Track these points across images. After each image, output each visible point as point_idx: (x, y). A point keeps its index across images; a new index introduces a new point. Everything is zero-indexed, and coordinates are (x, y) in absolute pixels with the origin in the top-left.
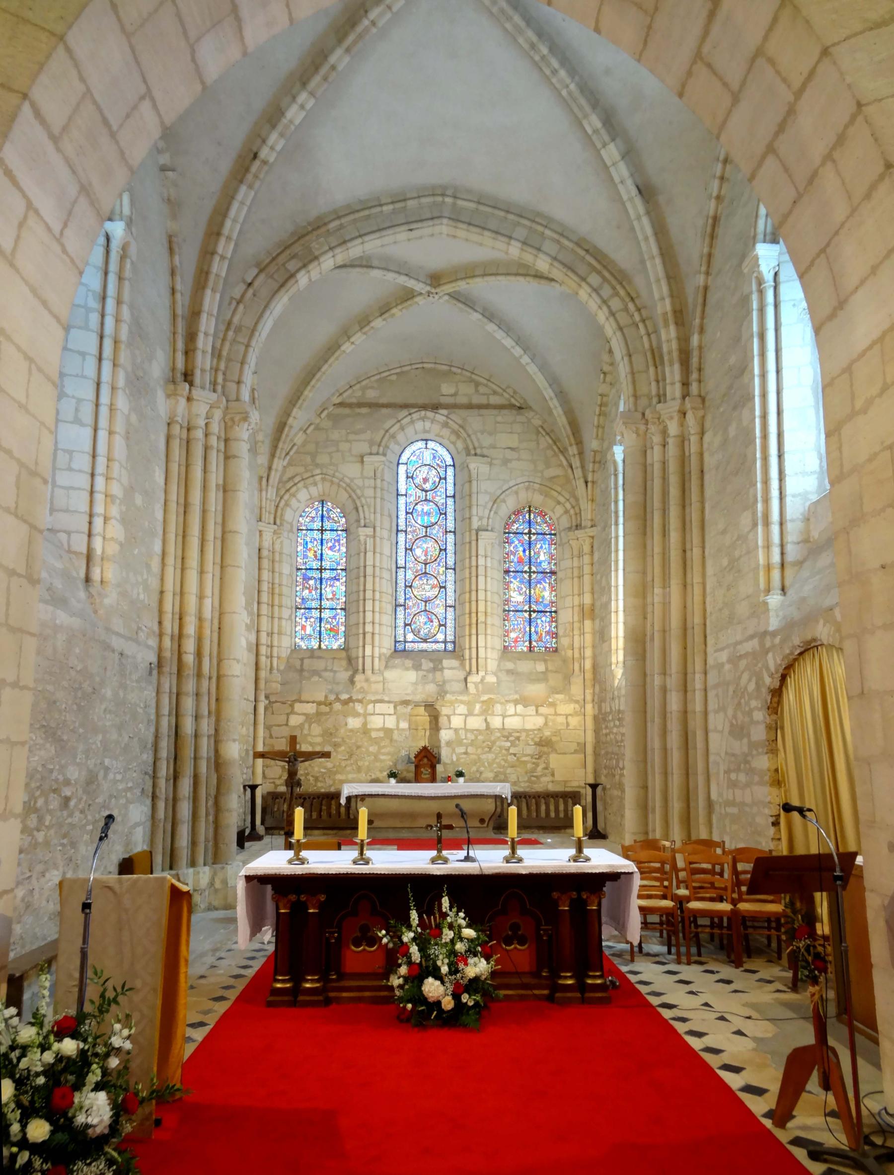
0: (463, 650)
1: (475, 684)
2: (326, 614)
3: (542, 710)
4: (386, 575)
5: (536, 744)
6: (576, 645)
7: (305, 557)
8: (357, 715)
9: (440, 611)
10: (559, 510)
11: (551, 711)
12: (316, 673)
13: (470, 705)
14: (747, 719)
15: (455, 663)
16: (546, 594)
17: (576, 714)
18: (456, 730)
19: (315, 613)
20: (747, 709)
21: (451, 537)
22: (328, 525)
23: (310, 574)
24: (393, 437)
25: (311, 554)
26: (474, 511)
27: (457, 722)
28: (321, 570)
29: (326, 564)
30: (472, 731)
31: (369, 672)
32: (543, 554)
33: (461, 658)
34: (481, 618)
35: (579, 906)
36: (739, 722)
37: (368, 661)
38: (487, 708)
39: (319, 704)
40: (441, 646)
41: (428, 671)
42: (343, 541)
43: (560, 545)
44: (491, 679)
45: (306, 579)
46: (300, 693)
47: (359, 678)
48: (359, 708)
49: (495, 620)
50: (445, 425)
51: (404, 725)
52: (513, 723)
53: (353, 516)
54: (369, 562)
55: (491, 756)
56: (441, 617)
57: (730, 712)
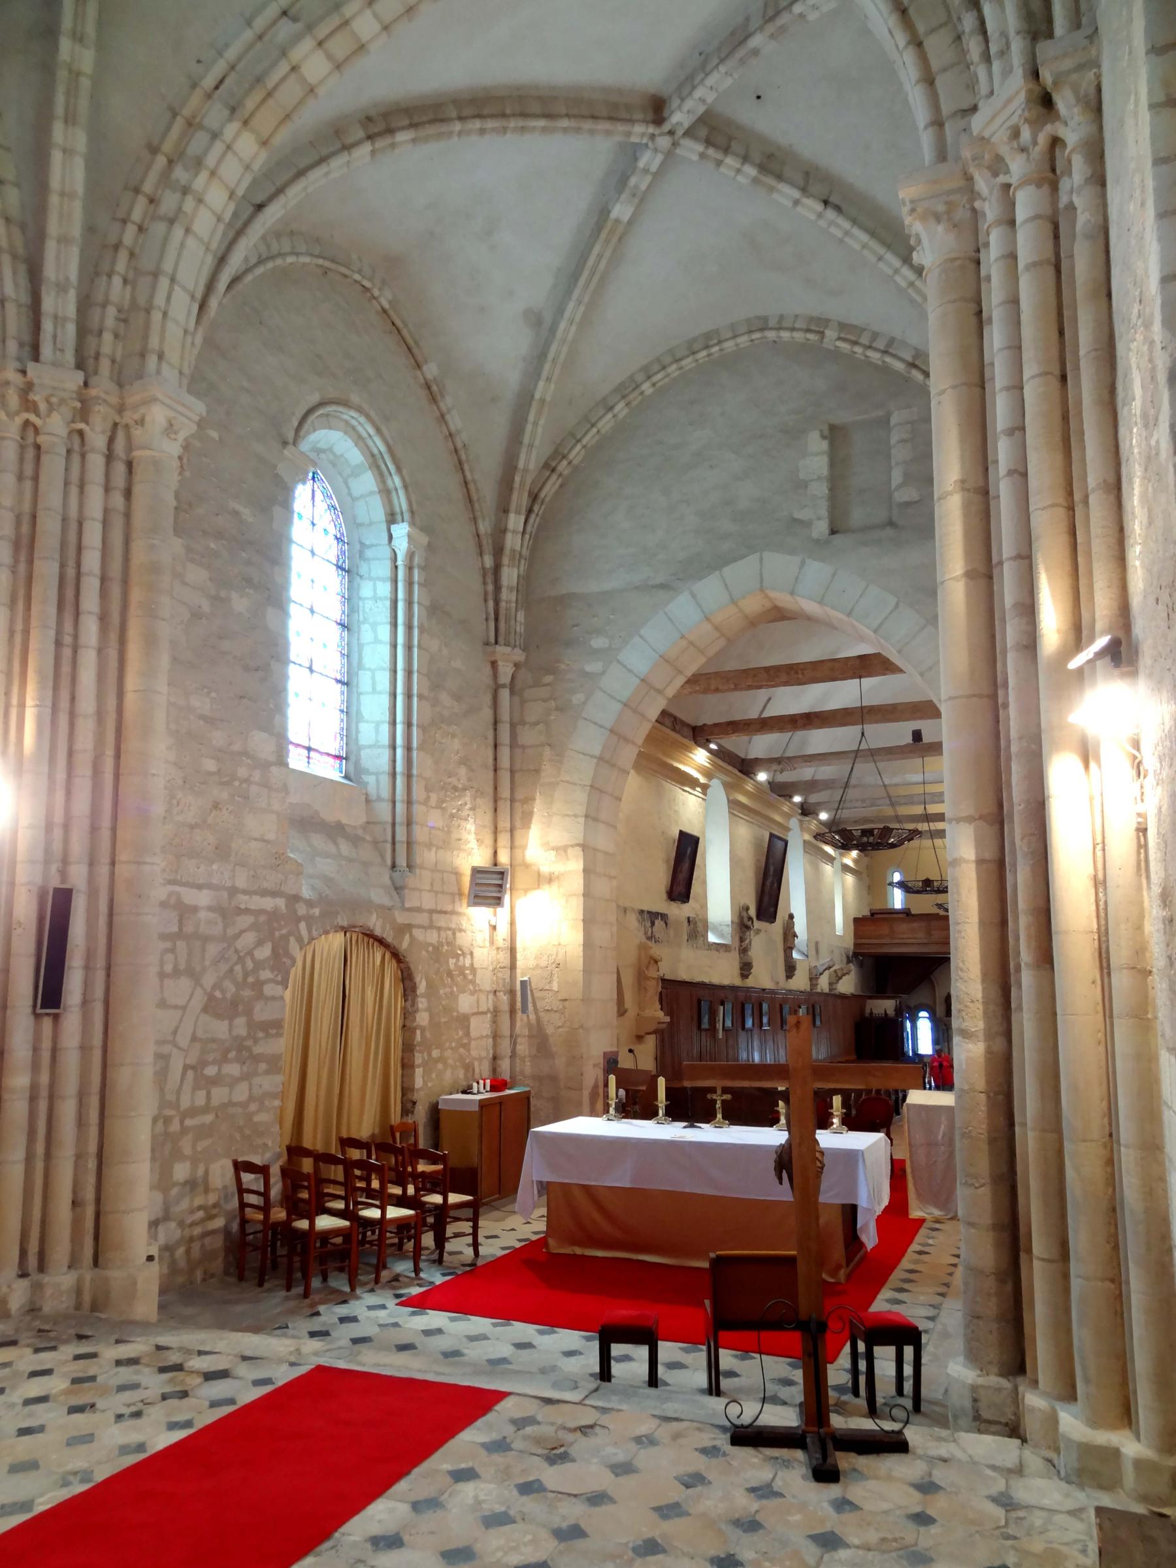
14: (247, 993)
20: (251, 979)
36: (229, 995)
57: (209, 980)
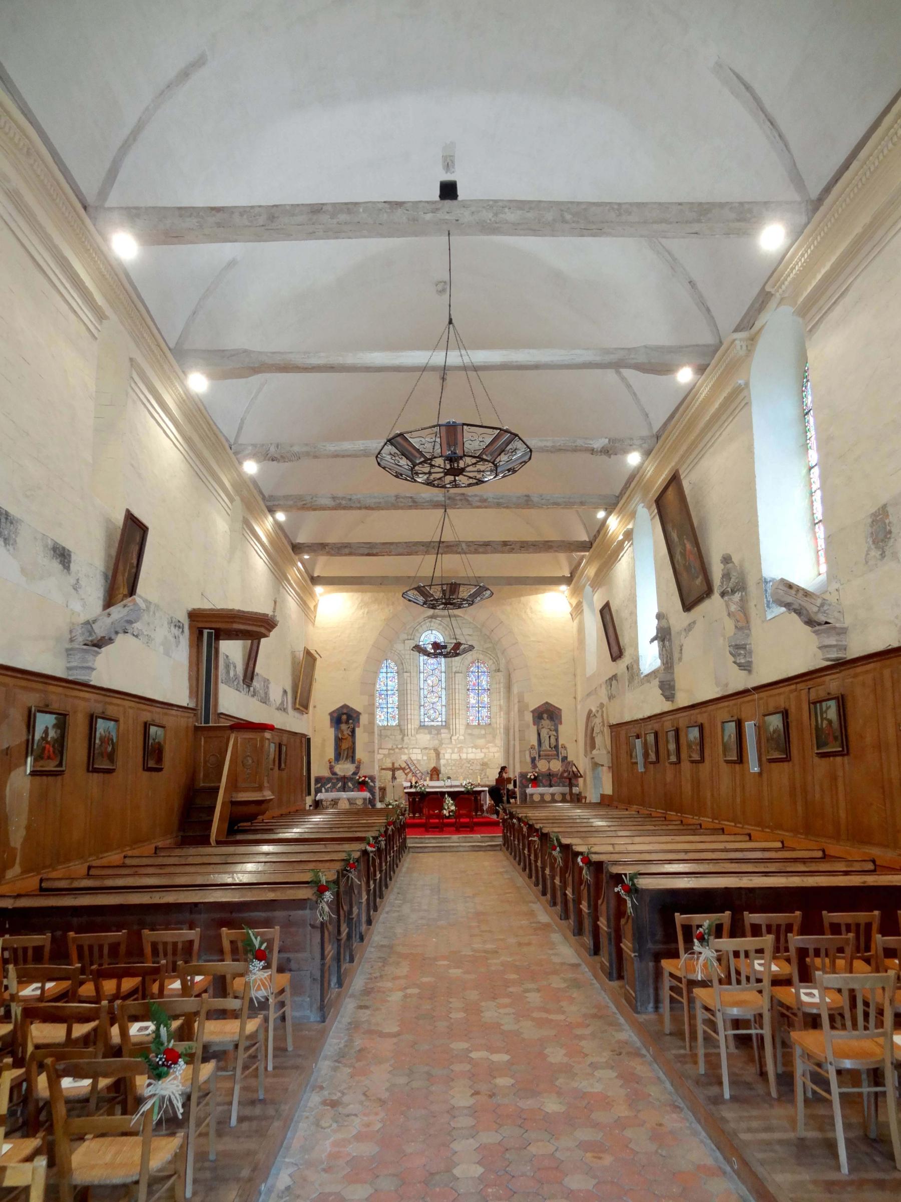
0: (449, 725)
1: (455, 740)
2: (390, 710)
3: (483, 750)
4: (416, 693)
5: (482, 765)
6: (498, 722)
7: (380, 685)
8: (406, 754)
9: (439, 708)
10: (491, 662)
11: (487, 751)
12: (386, 736)
13: (453, 749)
15: (446, 731)
16: (486, 699)
17: (497, 752)
18: (447, 760)
19: (385, 710)
21: (443, 675)
22: (389, 670)
23: (383, 692)
24: (417, 630)
25: (382, 684)
26: (453, 664)
27: (447, 756)
28: (387, 690)
29: (389, 688)
30: (454, 760)
31: (410, 736)
32: (484, 681)
33: (449, 729)
34: (457, 712)
35: (476, 798)
37: (409, 731)
38: (460, 750)
39: (389, 749)
40: (440, 724)
41: (435, 735)
42: (396, 677)
43: (492, 677)
44: (462, 738)
45: (380, 695)
46: (381, 745)
47: (406, 738)
48: (406, 751)
49: (464, 712)
50: (440, 624)
51: (425, 758)
52: (471, 756)
53: (401, 667)
54: (409, 688)
55: (462, 771)
56: (440, 710)
